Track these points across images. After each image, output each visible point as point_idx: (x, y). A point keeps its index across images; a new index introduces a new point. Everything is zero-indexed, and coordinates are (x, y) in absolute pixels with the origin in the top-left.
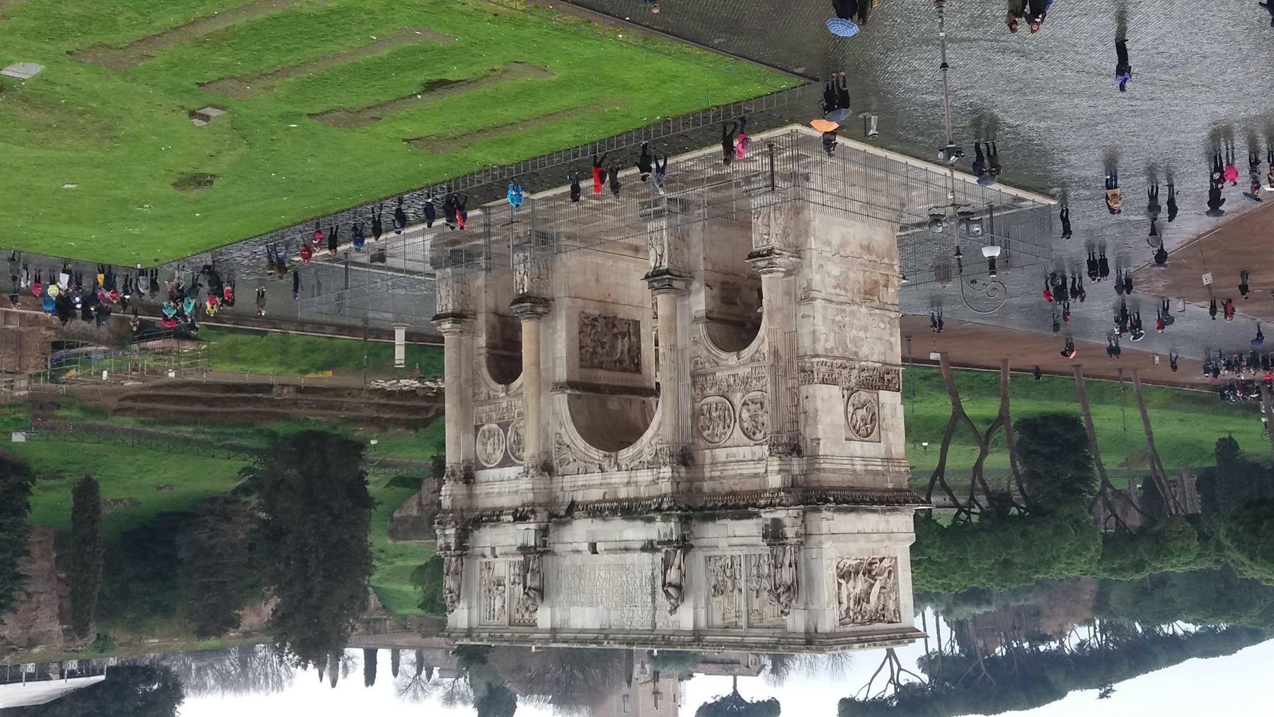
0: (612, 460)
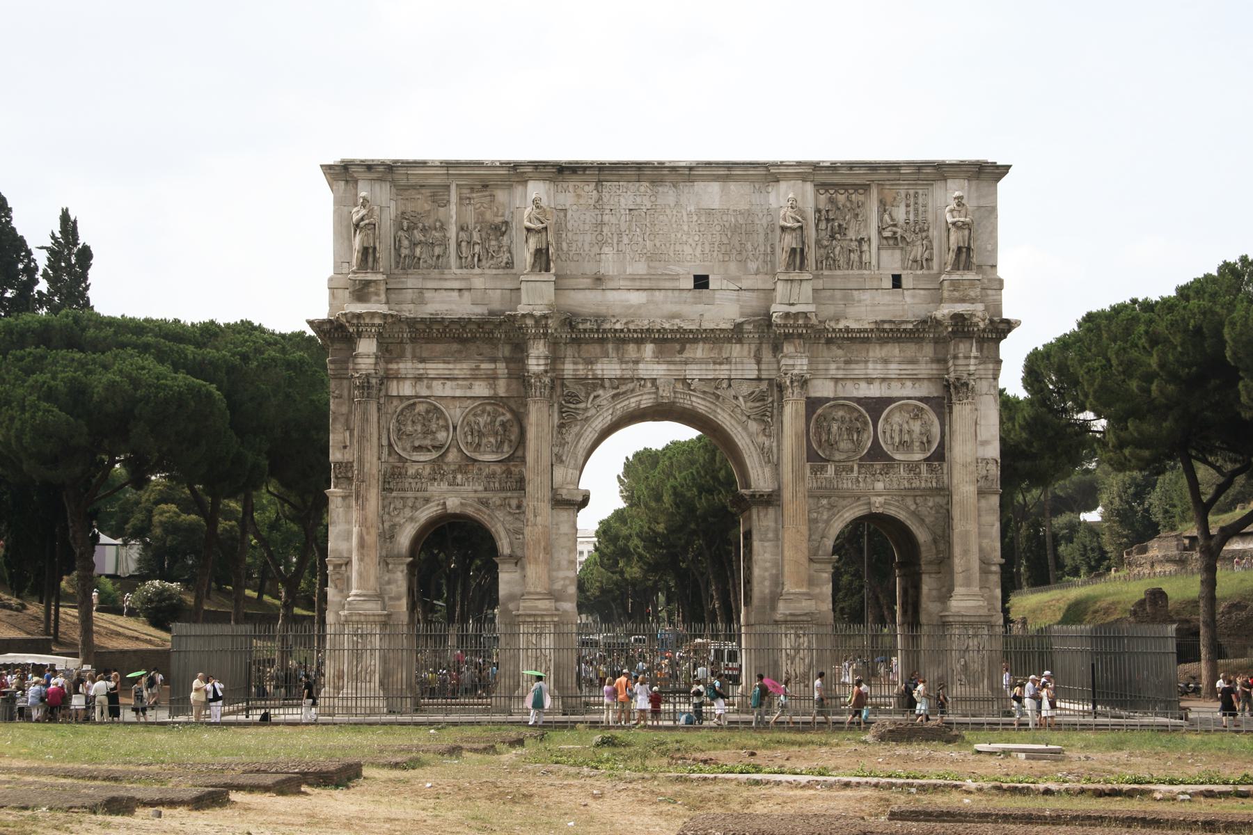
0: (661, 392)
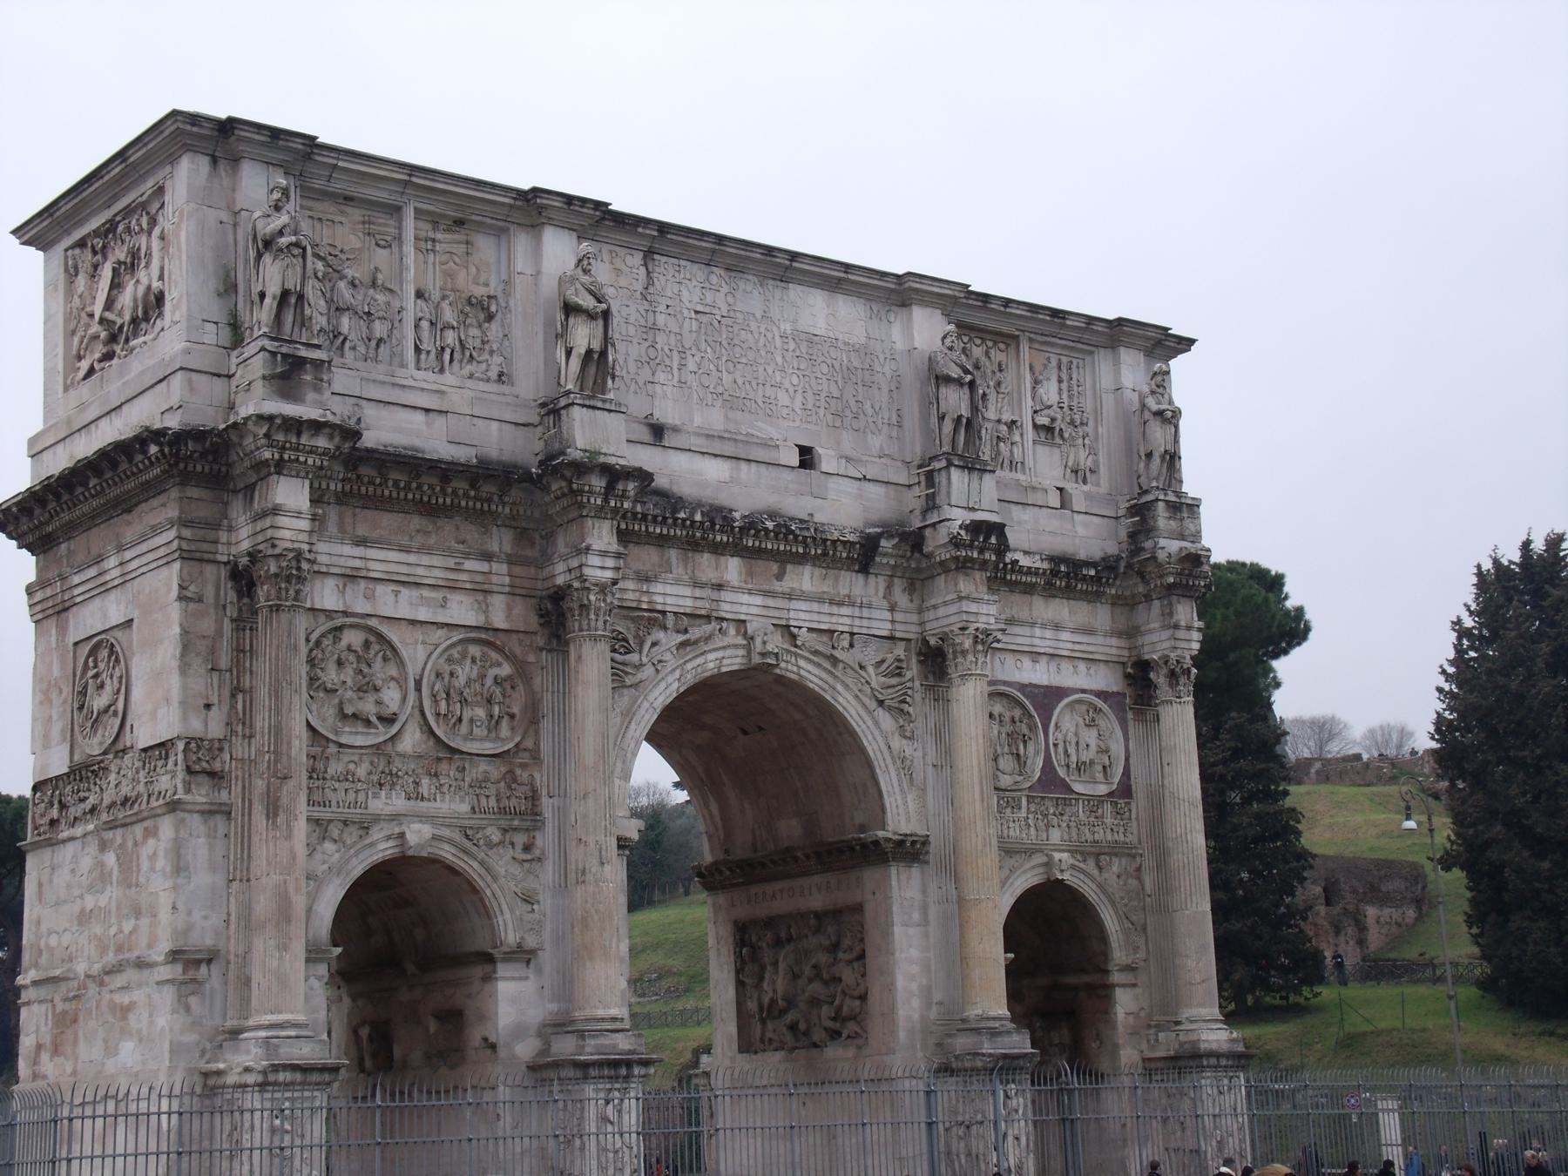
0: (758, 641)
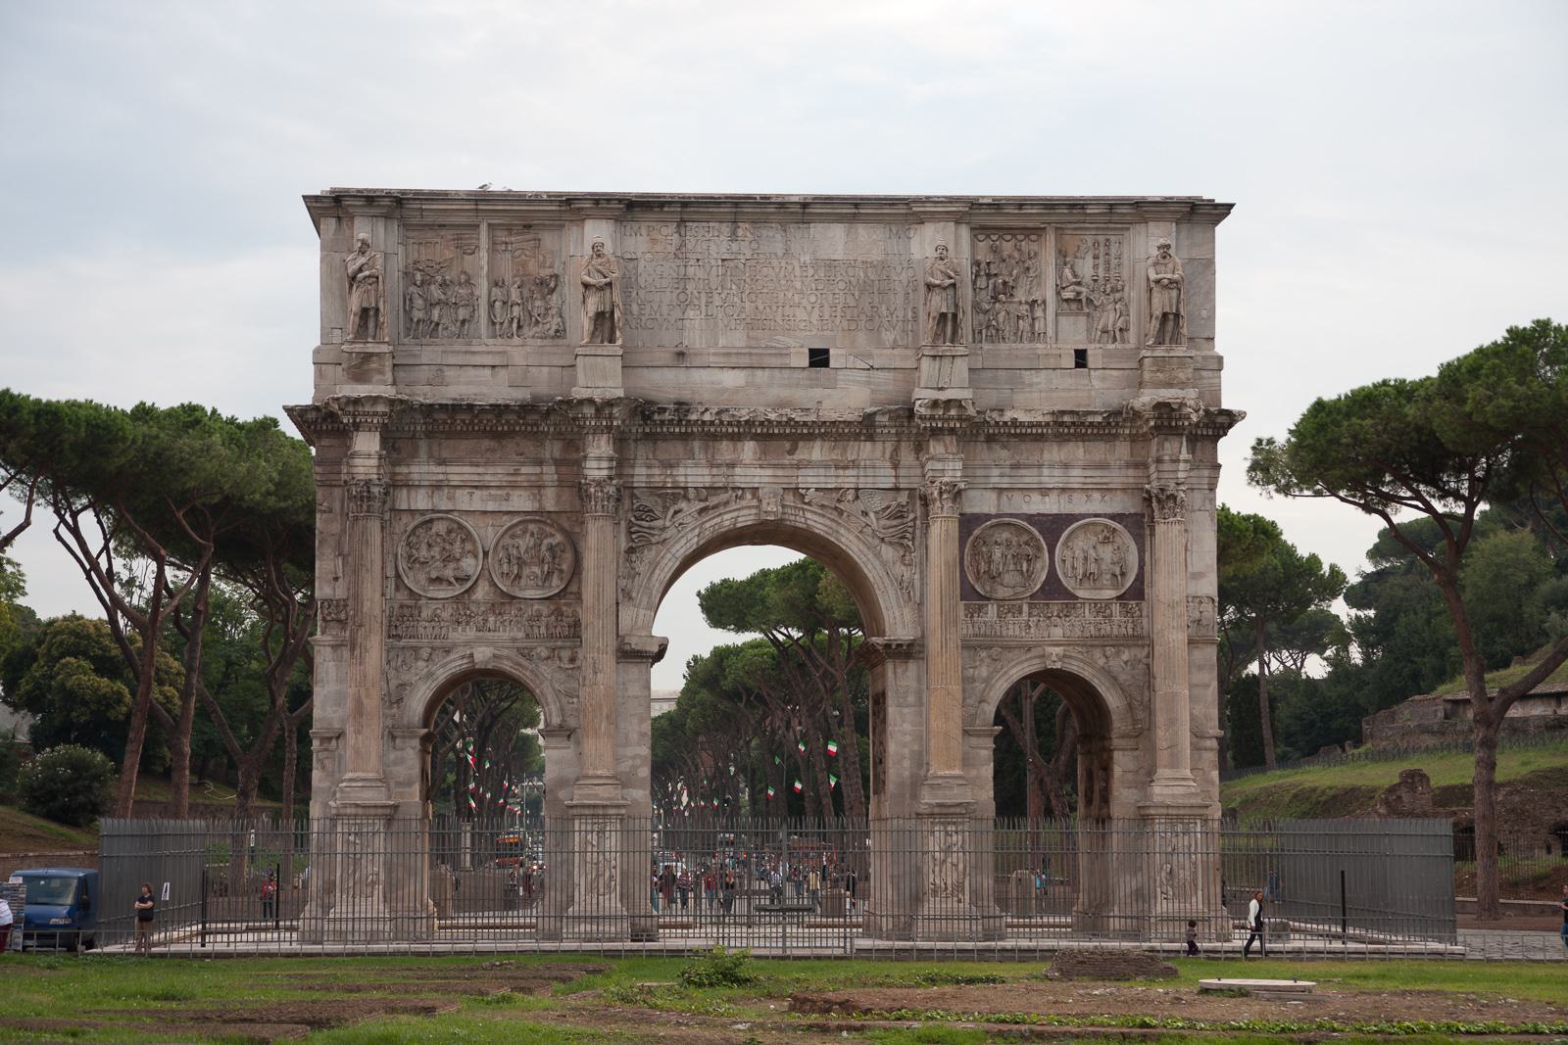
0: (764, 502)
